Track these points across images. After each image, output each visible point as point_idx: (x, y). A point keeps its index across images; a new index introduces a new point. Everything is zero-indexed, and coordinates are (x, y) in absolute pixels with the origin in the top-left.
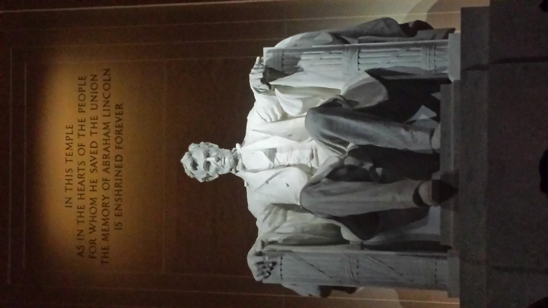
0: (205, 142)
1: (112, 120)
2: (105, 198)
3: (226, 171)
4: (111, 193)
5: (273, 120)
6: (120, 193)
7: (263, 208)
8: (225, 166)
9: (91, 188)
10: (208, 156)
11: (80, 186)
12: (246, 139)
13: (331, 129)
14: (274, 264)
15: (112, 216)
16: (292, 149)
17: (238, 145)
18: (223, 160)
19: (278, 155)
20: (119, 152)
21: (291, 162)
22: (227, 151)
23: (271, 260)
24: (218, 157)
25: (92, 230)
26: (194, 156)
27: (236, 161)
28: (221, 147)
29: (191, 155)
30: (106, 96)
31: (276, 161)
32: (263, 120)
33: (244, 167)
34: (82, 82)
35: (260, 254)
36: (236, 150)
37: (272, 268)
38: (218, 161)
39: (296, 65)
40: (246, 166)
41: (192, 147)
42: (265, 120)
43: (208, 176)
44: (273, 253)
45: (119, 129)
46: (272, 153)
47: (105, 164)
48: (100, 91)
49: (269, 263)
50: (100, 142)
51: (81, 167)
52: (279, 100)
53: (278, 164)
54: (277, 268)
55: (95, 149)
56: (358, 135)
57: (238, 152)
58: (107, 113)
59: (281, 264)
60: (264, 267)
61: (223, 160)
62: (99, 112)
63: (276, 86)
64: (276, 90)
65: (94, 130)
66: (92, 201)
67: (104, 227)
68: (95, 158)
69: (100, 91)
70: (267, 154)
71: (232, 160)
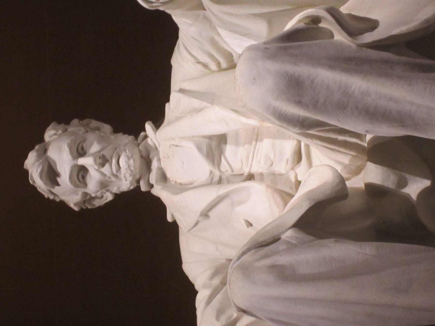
3: (125, 185)
5: (224, 65)
7: (209, 273)
8: (122, 176)
10: (81, 152)
12: (171, 109)
18: (114, 161)
21: (255, 169)
22: (125, 139)
26: (52, 153)
27: (147, 162)
28: (116, 130)
29: (46, 151)
31: (224, 166)
32: (200, 67)
36: (146, 137)
38: (103, 165)
40: (169, 175)
42: (205, 66)
43: (88, 198)
46: (215, 147)
56: (373, 114)
57: (149, 140)
61: (114, 161)
70: (205, 149)
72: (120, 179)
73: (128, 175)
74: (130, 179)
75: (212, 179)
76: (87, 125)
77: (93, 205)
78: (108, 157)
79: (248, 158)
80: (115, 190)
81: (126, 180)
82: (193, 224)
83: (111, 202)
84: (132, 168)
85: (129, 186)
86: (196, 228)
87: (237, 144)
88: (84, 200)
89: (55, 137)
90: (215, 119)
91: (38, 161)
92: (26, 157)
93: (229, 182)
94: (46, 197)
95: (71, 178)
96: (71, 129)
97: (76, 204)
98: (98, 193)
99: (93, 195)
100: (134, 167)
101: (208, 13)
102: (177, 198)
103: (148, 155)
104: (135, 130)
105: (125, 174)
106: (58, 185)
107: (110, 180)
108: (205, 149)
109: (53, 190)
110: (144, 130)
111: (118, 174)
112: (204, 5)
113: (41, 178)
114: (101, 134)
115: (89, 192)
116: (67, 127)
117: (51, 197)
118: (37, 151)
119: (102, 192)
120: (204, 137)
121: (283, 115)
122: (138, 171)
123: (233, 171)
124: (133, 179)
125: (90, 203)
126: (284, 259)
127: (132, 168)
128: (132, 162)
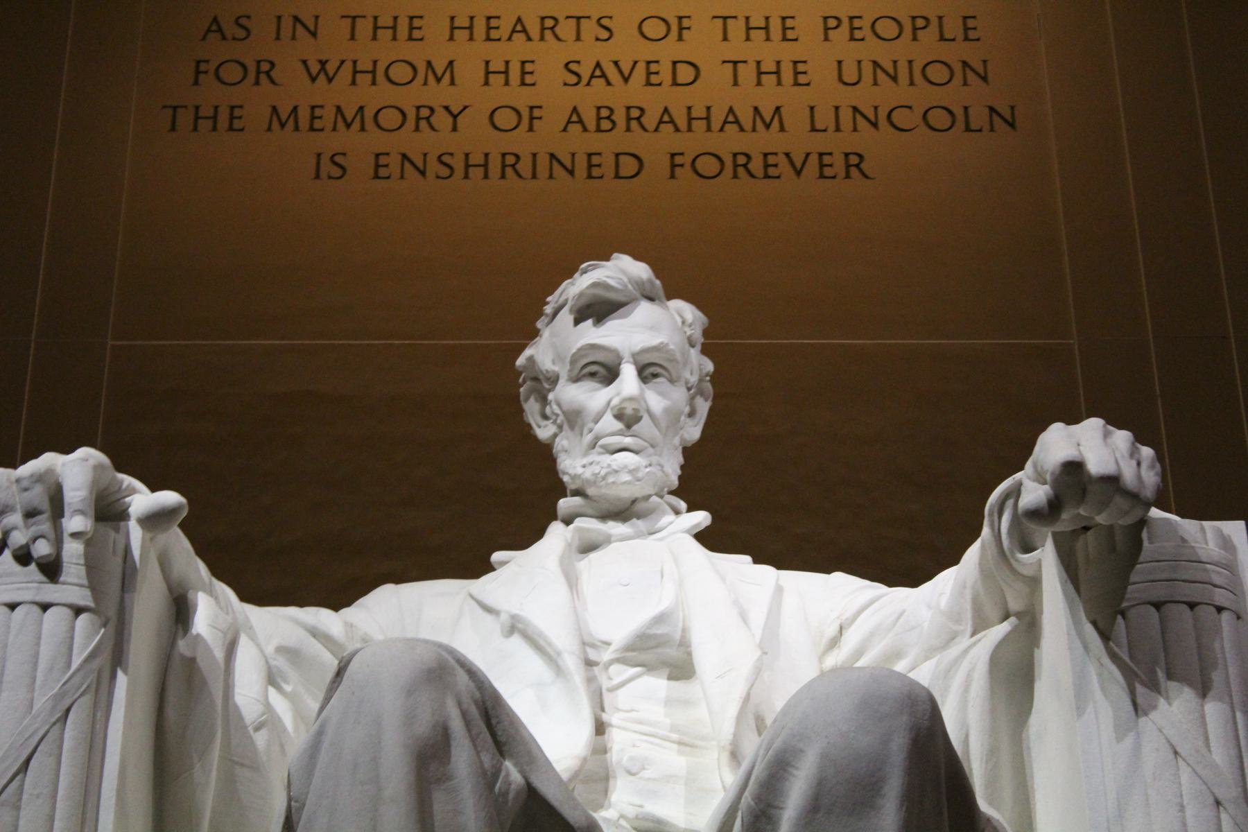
0: (715, 378)
1: (798, 140)
2: (455, 117)
4: (473, 136)
6: (476, 173)
8: (593, 457)
9: (497, 65)
10: (647, 372)
11: (506, 25)
13: (815, 807)
14: (52, 570)
15: (375, 140)
16: (686, 744)
17: (701, 518)
18: (628, 441)
19: (657, 685)
20: (657, 163)
21: (617, 739)
22: (671, 468)
23: (73, 550)
24: (638, 419)
25: (315, 68)
26: (644, 311)
27: (622, 512)
28: (689, 452)
29: (651, 299)
30: (899, 117)
31: (620, 673)
32: (832, 630)
33: (588, 547)
34: (953, 28)
35: (108, 511)
36: (677, 512)
37: (24, 557)
38: (619, 416)
39: (1170, 676)
40: (593, 556)
41: (684, 312)
42: (834, 642)
43: (543, 384)
44: (116, 564)
45: (756, 166)
46: (664, 653)
47: (605, 116)
48: (922, 96)
49: (58, 543)
50: (697, 97)
51: (589, 28)
52: (954, 651)
53: (605, 684)
54: (28, 584)
55: (666, 76)
57: (670, 517)
58: (824, 118)
59: (45, 607)
60: (30, 514)
61: (628, 441)
62: (825, 92)
63: (1029, 624)
64: (1001, 630)
65: (747, 73)
66: (439, 68)
67: (328, 114)
68: (626, 80)
69: (922, 96)
70: (660, 630)
71: (623, 489)
72: (586, 454)
73: (596, 469)
74: (587, 474)
75: (593, 646)
76: (701, 392)
77: (527, 399)
78: (635, 428)
79: (640, 723)
80: (561, 443)
81: (584, 466)
82: (490, 602)
83: (535, 438)
84: (611, 479)
85: (571, 472)
86: (479, 611)
87: (669, 702)
88: (541, 377)
89: (679, 320)
90: (724, 659)
91: (630, 281)
92: (637, 257)
93: (590, 680)
94: (549, 299)
95: (594, 347)
96: (694, 354)
97: (531, 359)
98: (555, 407)
99: (551, 396)
100: (613, 483)
101: (965, 641)
102: (553, 564)
103: (639, 516)
104: (691, 488)
105: (598, 463)
106: (577, 322)
107: (585, 431)
108: (659, 632)
109: (566, 308)
110: (689, 510)
111: (597, 449)
112: (983, 633)
113: (595, 285)
114: (683, 418)
115: (558, 387)
116: (699, 347)
117: (548, 309)
118: (650, 281)
119: (557, 415)
120: (684, 630)
121: (785, 771)
122: (603, 491)
123: (611, 690)
124: (588, 481)
125: (531, 392)
126: (463, 759)
127: (611, 479)
128: (626, 477)
